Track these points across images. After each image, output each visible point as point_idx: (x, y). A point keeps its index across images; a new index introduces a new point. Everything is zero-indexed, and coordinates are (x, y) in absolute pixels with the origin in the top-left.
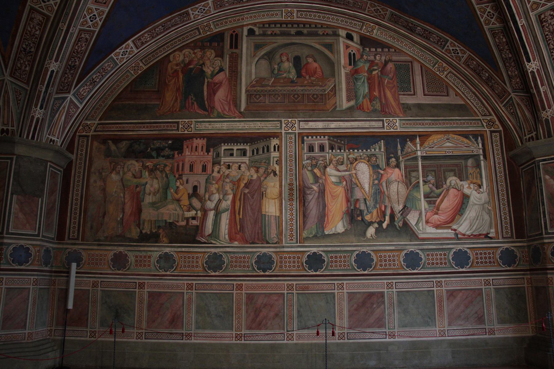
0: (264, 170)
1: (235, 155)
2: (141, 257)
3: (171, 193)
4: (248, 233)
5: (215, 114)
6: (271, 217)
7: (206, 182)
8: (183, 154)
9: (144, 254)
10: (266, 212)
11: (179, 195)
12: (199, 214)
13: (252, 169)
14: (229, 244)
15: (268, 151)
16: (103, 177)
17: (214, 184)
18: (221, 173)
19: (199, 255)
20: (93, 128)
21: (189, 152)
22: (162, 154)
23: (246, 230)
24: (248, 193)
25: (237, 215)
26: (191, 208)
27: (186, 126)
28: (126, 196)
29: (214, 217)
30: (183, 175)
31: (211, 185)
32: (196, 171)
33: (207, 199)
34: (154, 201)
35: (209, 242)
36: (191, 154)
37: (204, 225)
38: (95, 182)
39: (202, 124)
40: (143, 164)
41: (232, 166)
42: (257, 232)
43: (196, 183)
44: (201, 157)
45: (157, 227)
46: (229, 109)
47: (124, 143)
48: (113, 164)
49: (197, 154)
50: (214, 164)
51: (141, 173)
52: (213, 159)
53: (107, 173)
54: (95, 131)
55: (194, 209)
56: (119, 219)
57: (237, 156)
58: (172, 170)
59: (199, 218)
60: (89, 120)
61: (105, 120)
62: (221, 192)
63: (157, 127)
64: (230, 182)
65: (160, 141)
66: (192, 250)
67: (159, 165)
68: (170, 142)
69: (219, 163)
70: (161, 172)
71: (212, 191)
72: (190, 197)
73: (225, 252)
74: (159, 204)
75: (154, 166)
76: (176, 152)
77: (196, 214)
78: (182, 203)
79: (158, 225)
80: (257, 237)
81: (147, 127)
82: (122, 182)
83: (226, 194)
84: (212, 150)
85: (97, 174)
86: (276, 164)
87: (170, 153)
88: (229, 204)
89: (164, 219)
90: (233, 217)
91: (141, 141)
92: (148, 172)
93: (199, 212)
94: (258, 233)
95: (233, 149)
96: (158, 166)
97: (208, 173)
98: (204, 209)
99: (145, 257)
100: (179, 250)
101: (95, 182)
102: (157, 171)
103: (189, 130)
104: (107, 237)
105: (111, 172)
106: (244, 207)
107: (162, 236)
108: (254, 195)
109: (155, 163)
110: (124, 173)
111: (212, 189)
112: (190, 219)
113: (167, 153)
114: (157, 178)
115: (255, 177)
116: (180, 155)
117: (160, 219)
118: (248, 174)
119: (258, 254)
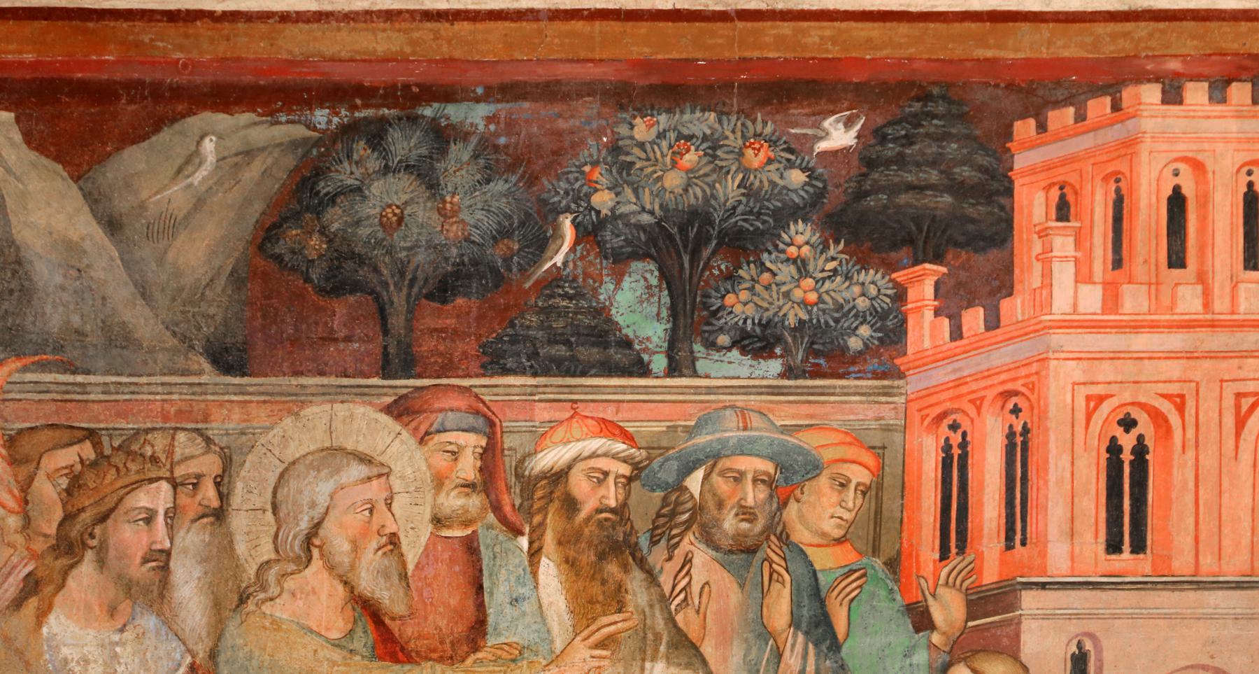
8: (1014, 308)
21: (1083, 277)
30: (1030, 601)
32: (1184, 541)
36: (1112, 299)
40: (490, 456)
48: (68, 457)
49: (1189, 301)
65: (701, 122)
67: (712, 458)
75: (638, 468)
92: (570, 563)
96: (694, 482)
102: (690, 543)
105: (32, 586)
109: (647, 427)
113: (806, 290)
116: (974, 319)
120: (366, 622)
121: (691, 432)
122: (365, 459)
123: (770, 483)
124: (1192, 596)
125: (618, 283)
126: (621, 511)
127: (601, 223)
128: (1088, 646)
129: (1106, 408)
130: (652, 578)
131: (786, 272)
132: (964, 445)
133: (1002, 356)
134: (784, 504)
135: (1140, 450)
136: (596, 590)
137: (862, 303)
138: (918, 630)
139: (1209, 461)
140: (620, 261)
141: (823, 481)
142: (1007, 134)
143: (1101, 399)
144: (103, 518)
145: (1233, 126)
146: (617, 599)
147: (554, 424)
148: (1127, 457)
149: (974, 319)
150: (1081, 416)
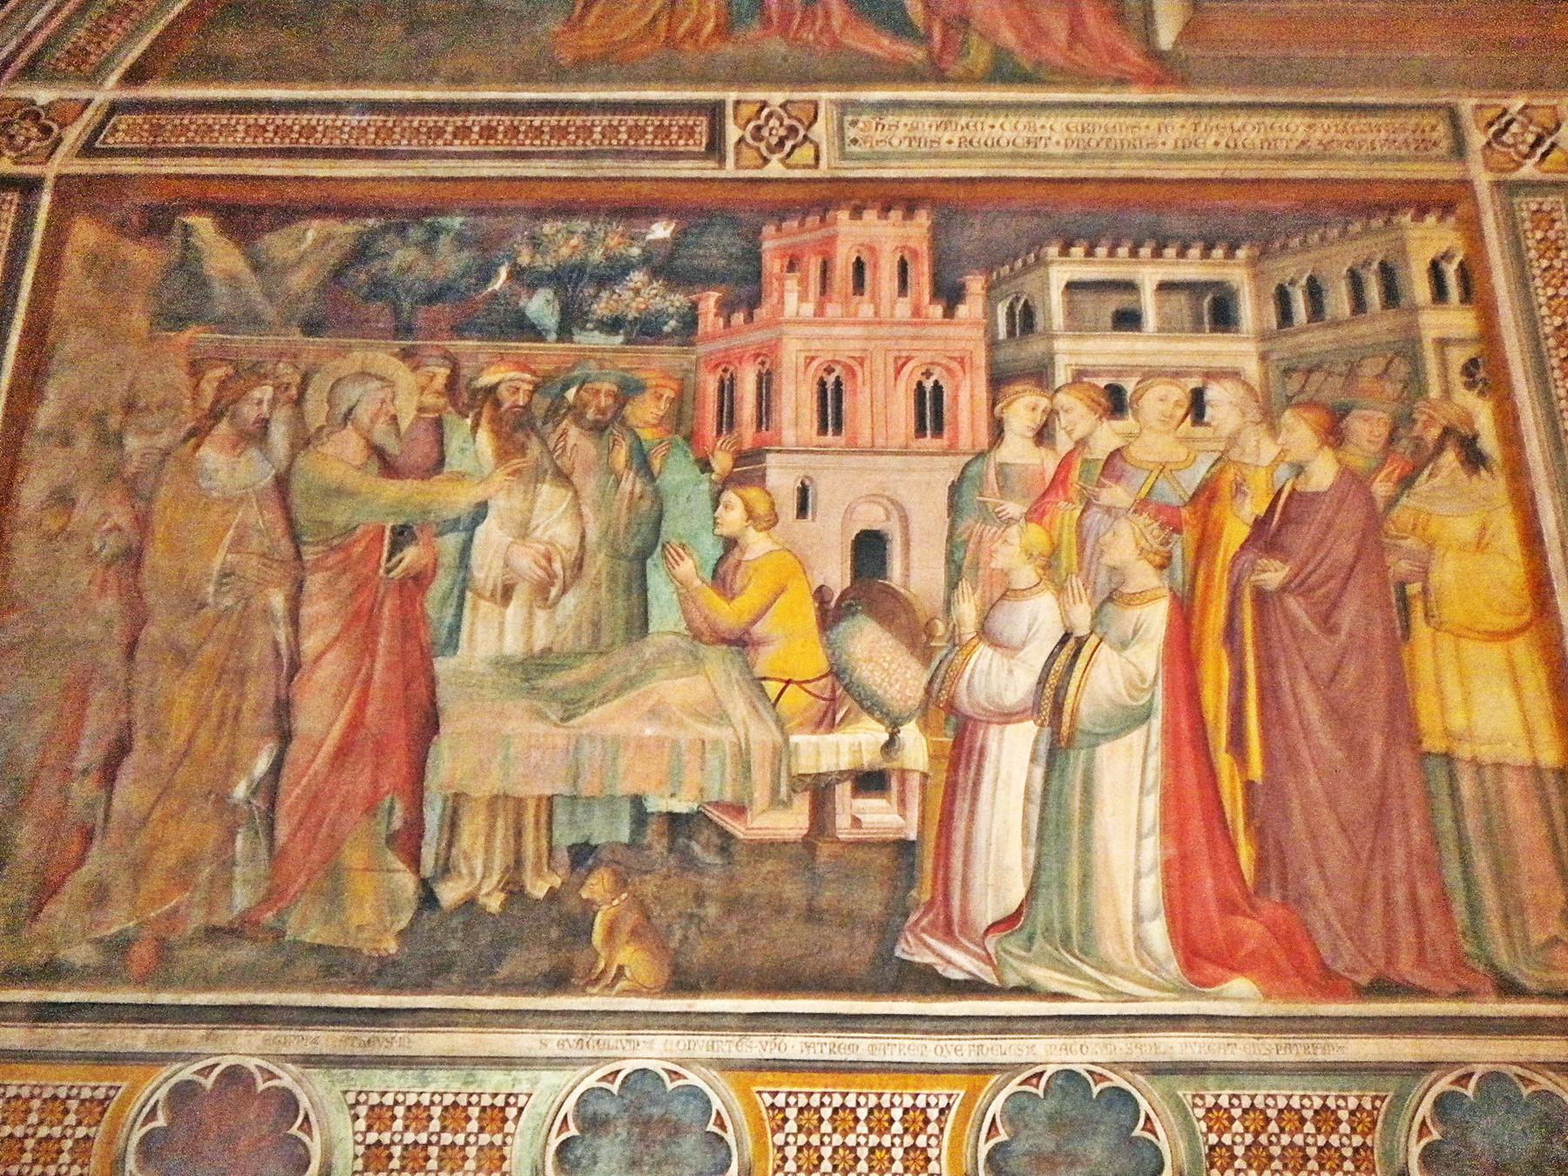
0: (1383, 431)
1: (1150, 319)
2: (418, 1115)
3: (681, 585)
4: (1327, 906)
5: (979, 56)
6: (1499, 781)
7: (954, 508)
8: (762, 313)
9: (444, 1082)
10: (1447, 733)
11: (747, 602)
12: (916, 748)
13: (1288, 417)
14: (1182, 993)
15: (1392, 295)
16: (131, 469)
17: (1009, 522)
18: (1064, 444)
19: (935, 1094)
20: (73, 135)
21: (803, 298)
22: (602, 307)
23: (1313, 880)
24: (1284, 588)
25: (1224, 761)
26: (849, 703)
27: (775, 129)
28: (306, 612)
29: (1039, 772)
30: (771, 459)
31: (991, 530)
33: (969, 628)
34: (537, 648)
35: (1013, 980)
36: (820, 311)
37: (959, 837)
38: (62, 499)
39: (889, 119)
41: (1138, 393)
42: (1400, 894)
43: (881, 511)
44: (902, 331)
45: (563, 857)
46: (1076, 31)
47: (313, 230)
50: (999, 381)
51: (440, 442)
52: (993, 344)
53: (163, 440)
54: (88, 150)
55: (871, 705)
56: (240, 791)
57: (1167, 327)
58: (680, 419)
59: (914, 781)
60: (52, 78)
61: (173, 78)
62: (1077, 582)
63: (560, 132)
64: (1141, 505)
65: (581, 225)
66: (862, 1047)
68: (661, 231)
69: (1040, 375)
70: (598, 429)
71: (1005, 574)
72: (830, 613)
73: (1155, 1070)
74: (586, 669)
76: (710, 301)
77: (890, 746)
78: (765, 662)
79: (574, 838)
80: (1406, 934)
81: (488, 132)
82: (286, 509)
83: (1113, 597)
84: (975, 284)
85: (84, 443)
86: (1470, 386)
87: (658, 304)
88: (1150, 678)
89: (625, 787)
90: (1190, 774)
91: (445, 221)
92: (497, 434)
93: (910, 733)
94: (1413, 898)
95: (1129, 286)
96: (571, 394)
97: (965, 441)
98: (951, 707)
99: (455, 1113)
100: (757, 1046)
101: (62, 499)
103: (798, 156)
104: (119, 946)
105: (192, 433)
106: (1268, 694)
107: (611, 931)
108: (1335, 605)
110: (303, 441)
111: (998, 562)
112: (844, 790)
113: (639, 303)
114: (563, 477)
115: (1323, 472)
116: (739, 318)
117: (587, 787)
118: (1269, 450)
119: (1444, 1085)
120: (375, 458)
121: (569, 370)
122: (382, 379)
123: (616, 397)
124: (870, 458)
125: (530, 298)
126: (527, 407)
127: (523, 270)
128: (807, 482)
129: (815, 364)
130: (544, 441)
131: (628, 295)
132: (732, 379)
133: (756, 337)
134: (623, 406)
135: (838, 383)
136: (510, 447)
137: (671, 310)
138: (703, 472)
139: (880, 390)
140: (532, 288)
141: (647, 395)
142: (760, 232)
143: (813, 359)
144: (235, 402)
145: (891, 231)
146: (522, 450)
147: (490, 364)
148: (830, 387)
149: (739, 318)
150: (802, 368)
